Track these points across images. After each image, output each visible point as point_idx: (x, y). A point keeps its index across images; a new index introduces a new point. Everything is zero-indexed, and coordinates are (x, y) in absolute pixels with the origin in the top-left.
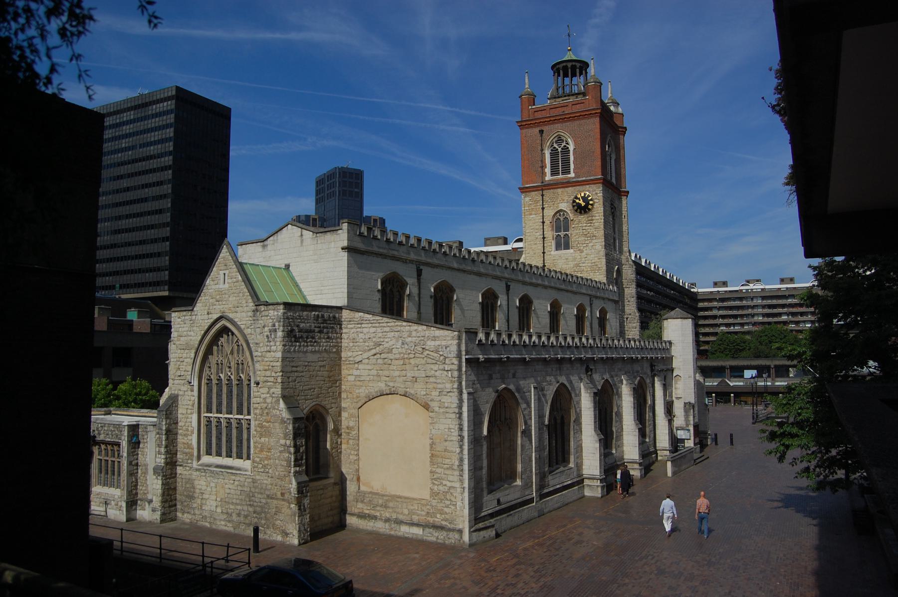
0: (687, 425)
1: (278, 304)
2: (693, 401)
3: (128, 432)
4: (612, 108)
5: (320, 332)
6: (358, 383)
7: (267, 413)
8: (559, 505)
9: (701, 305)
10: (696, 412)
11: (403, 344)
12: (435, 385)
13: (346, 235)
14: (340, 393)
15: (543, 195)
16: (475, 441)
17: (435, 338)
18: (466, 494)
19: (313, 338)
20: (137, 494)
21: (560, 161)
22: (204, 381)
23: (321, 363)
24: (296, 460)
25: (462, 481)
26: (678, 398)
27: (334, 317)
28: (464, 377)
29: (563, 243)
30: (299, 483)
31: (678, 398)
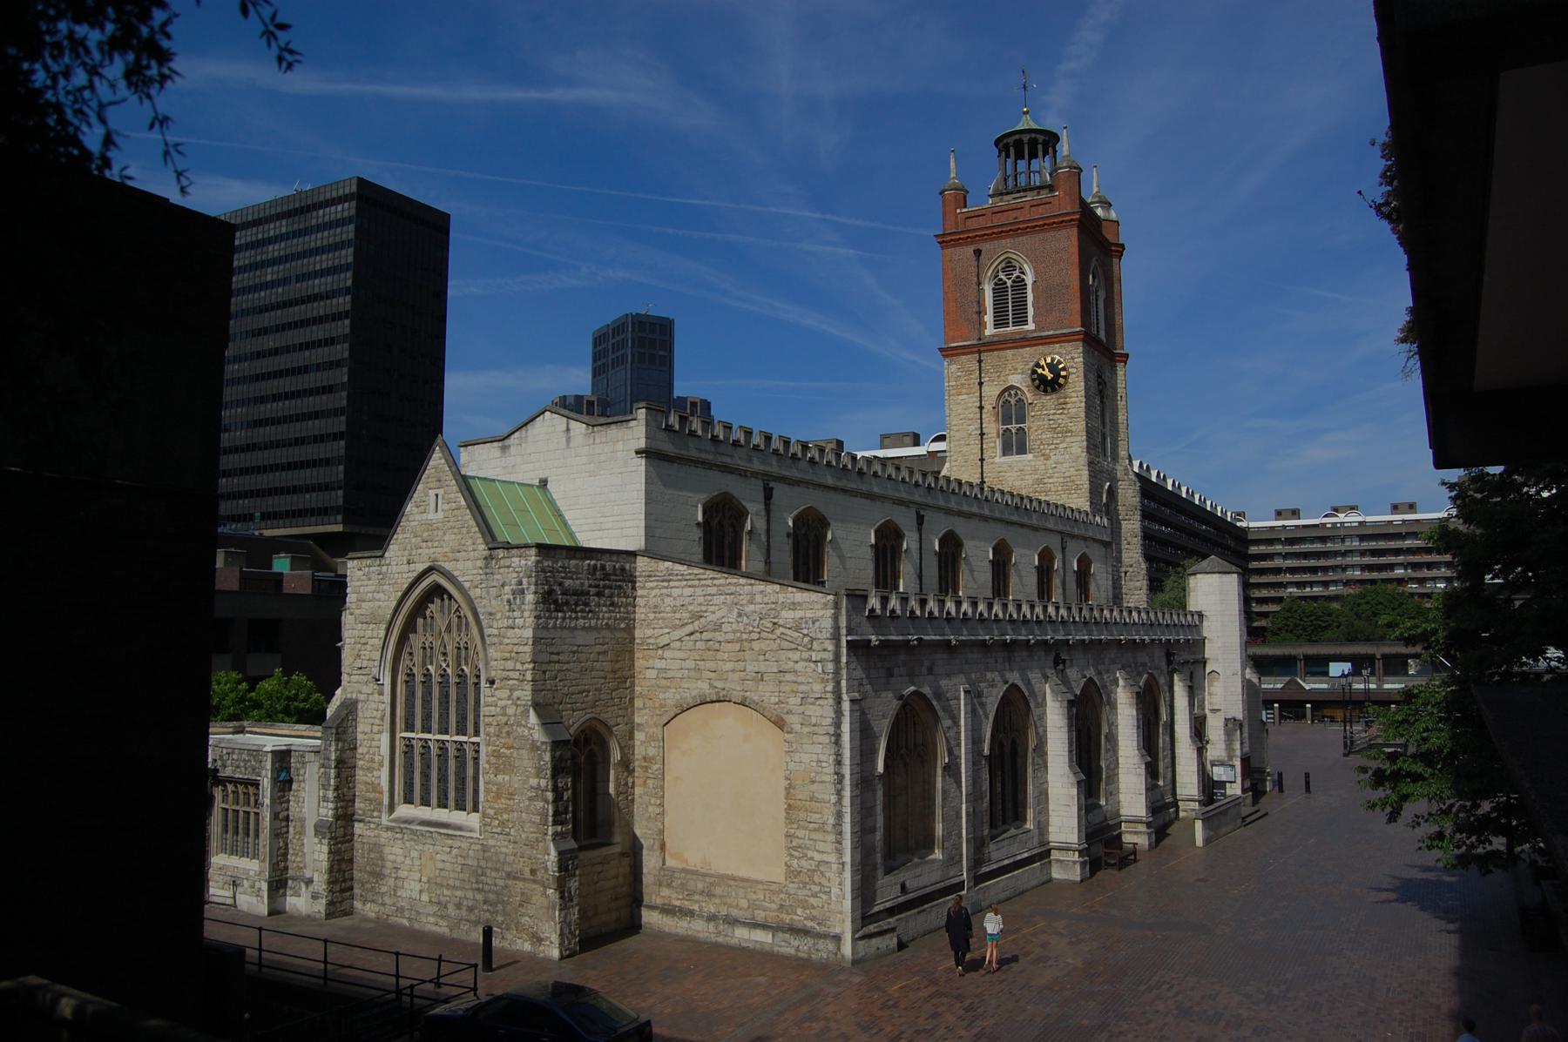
0: (1231, 757)
1: (527, 546)
2: (1240, 716)
3: (273, 763)
4: (1099, 212)
5: (599, 594)
6: (664, 682)
7: (508, 733)
8: (1007, 894)
10: (1246, 735)
11: (740, 615)
12: (795, 687)
13: (643, 429)
14: (632, 700)
15: (980, 361)
16: (864, 781)
17: (794, 606)
18: (848, 874)
19: (587, 604)
20: (286, 868)
21: (1010, 303)
22: (401, 678)
23: (599, 648)
24: (556, 814)
25: (840, 852)
26: (1213, 711)
27: (623, 569)
28: (844, 672)
29: (1015, 444)
30: (560, 853)
31: (1213, 711)
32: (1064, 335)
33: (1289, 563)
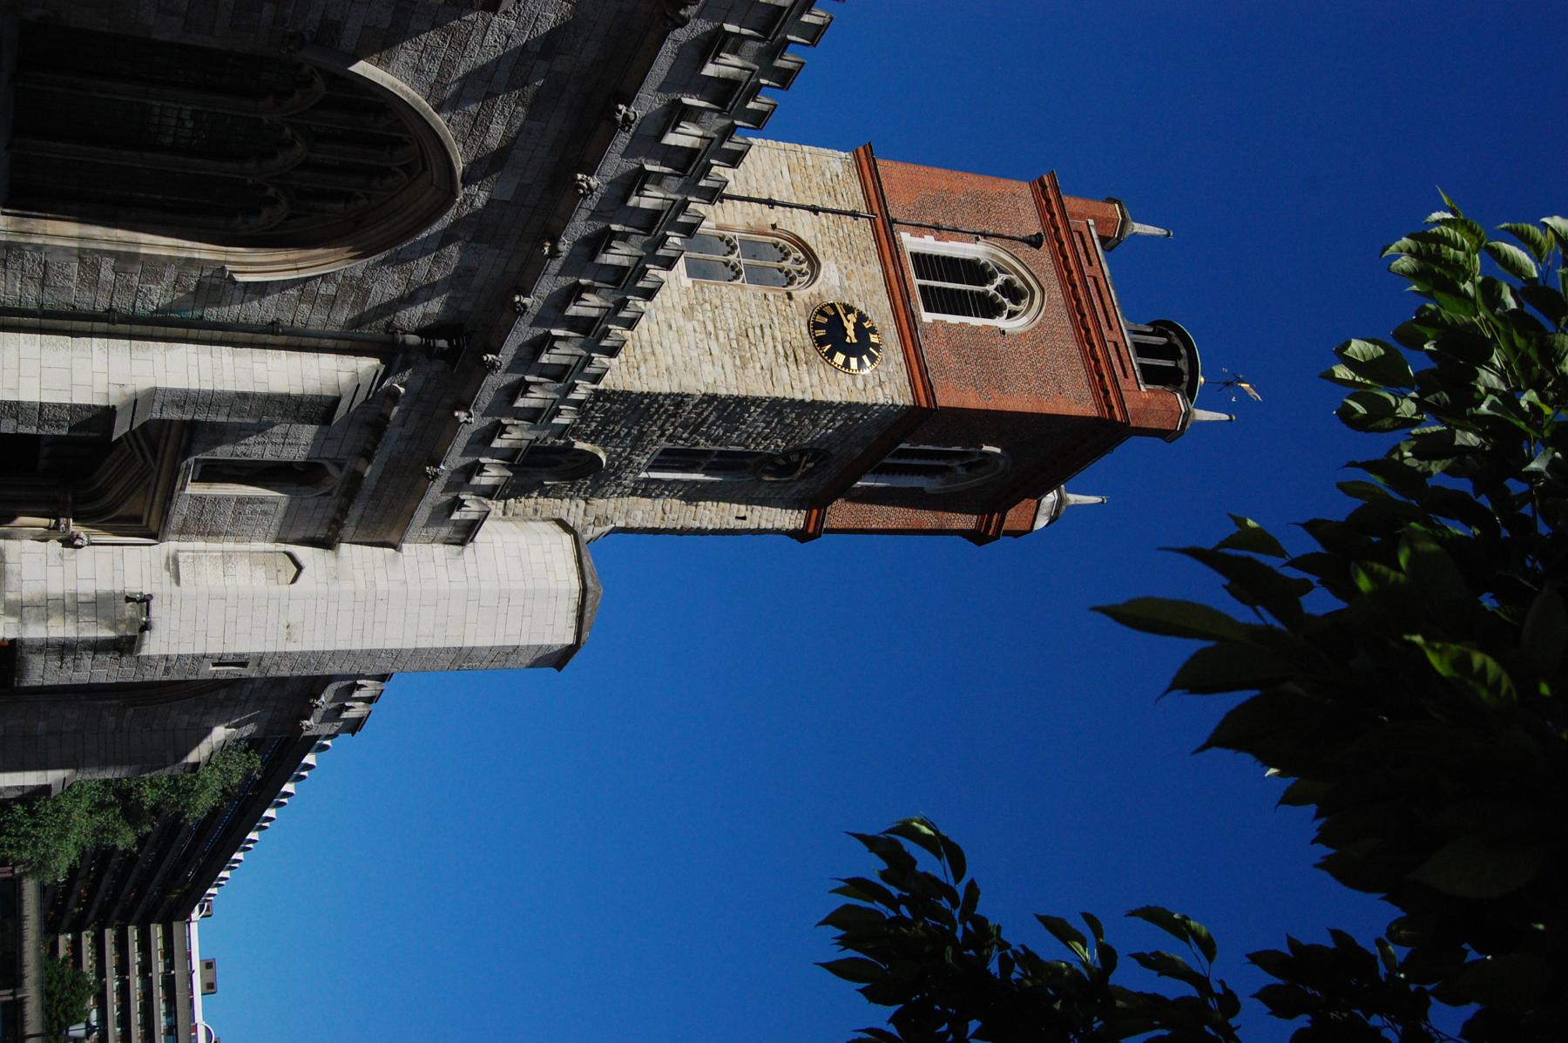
2: (153, 646)
4: (1051, 498)
9: (157, 931)
15: (854, 214)
26: (173, 565)
31: (173, 565)
32: (924, 371)
33: (136, 983)
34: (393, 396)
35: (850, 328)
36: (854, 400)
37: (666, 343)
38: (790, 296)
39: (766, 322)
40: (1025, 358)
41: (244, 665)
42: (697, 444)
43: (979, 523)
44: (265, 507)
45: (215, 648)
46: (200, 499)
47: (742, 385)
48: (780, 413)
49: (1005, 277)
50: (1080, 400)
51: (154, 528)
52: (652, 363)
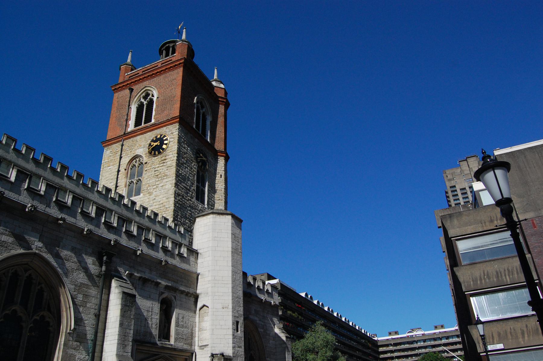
2: (229, 352)
4: (214, 83)
15: (122, 145)
26: (202, 347)
31: (202, 347)
32: (168, 120)
34: (130, 276)
35: (155, 144)
36: (177, 141)
37: (159, 200)
38: (146, 163)
39: (154, 170)
40: (166, 91)
41: (237, 322)
42: (194, 189)
43: (222, 104)
44: (180, 318)
45: (230, 332)
46: (176, 339)
47: (172, 176)
48: (182, 164)
49: (142, 99)
50: (178, 73)
51: (190, 354)
52: (165, 204)
